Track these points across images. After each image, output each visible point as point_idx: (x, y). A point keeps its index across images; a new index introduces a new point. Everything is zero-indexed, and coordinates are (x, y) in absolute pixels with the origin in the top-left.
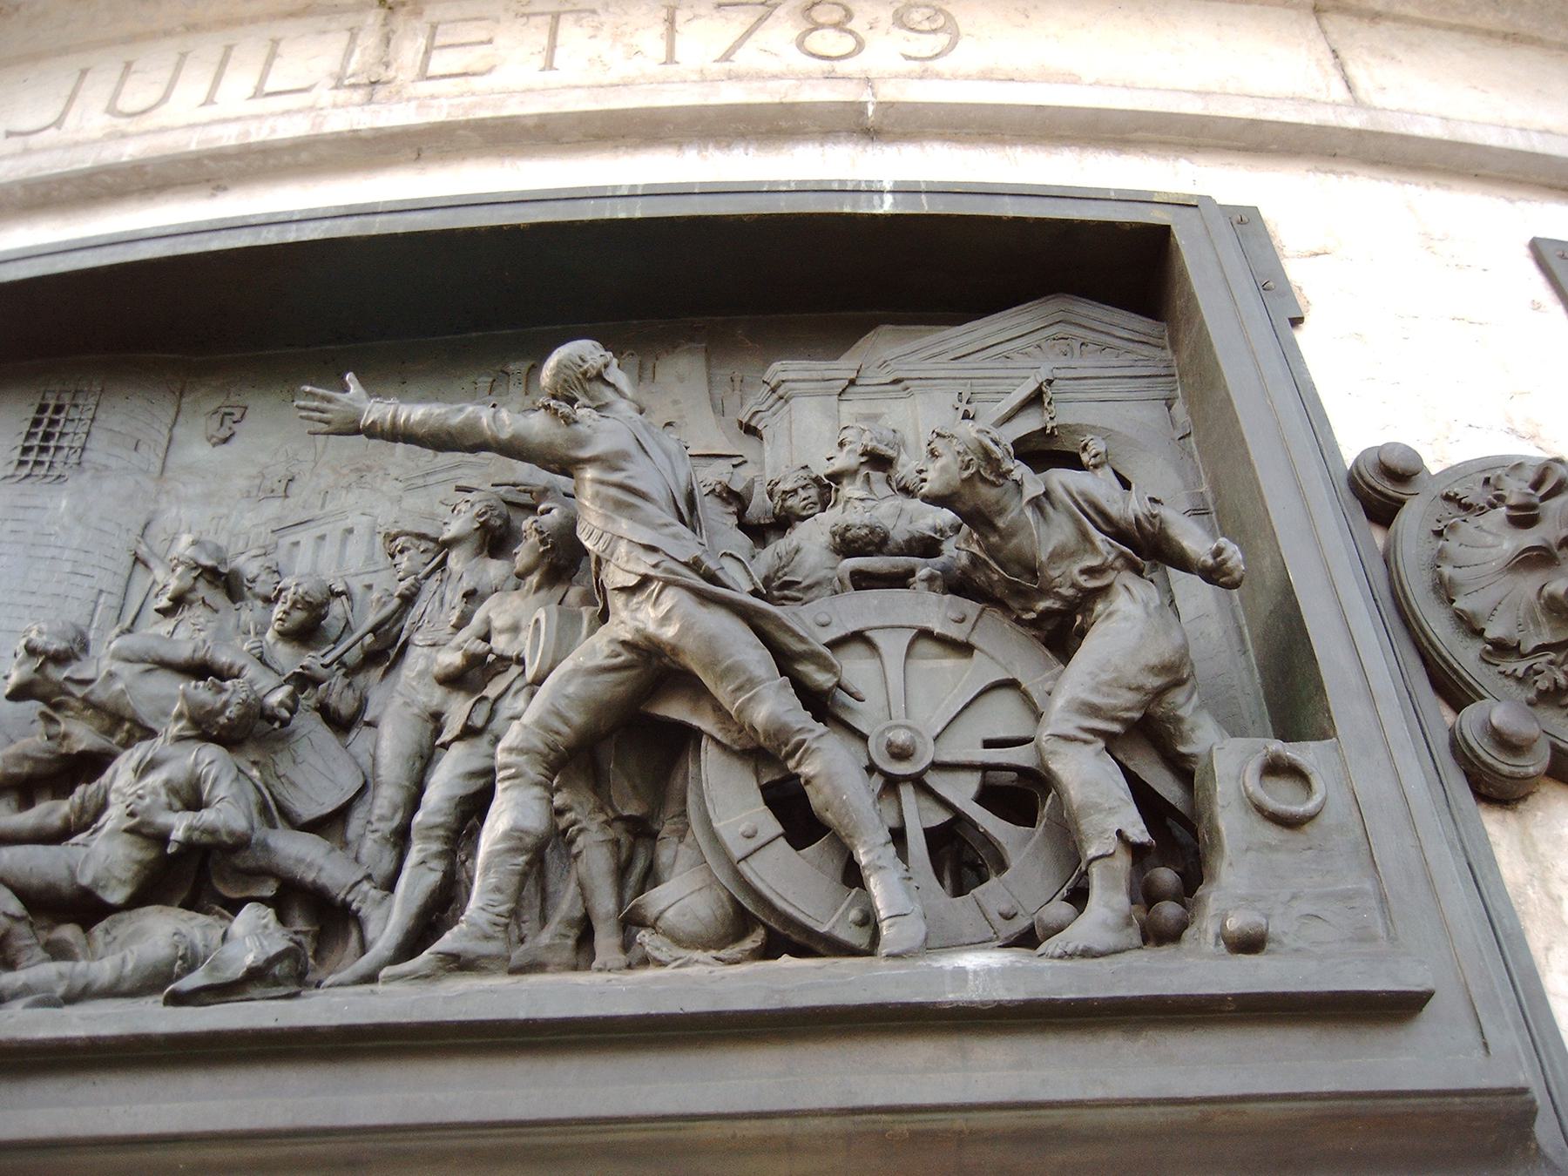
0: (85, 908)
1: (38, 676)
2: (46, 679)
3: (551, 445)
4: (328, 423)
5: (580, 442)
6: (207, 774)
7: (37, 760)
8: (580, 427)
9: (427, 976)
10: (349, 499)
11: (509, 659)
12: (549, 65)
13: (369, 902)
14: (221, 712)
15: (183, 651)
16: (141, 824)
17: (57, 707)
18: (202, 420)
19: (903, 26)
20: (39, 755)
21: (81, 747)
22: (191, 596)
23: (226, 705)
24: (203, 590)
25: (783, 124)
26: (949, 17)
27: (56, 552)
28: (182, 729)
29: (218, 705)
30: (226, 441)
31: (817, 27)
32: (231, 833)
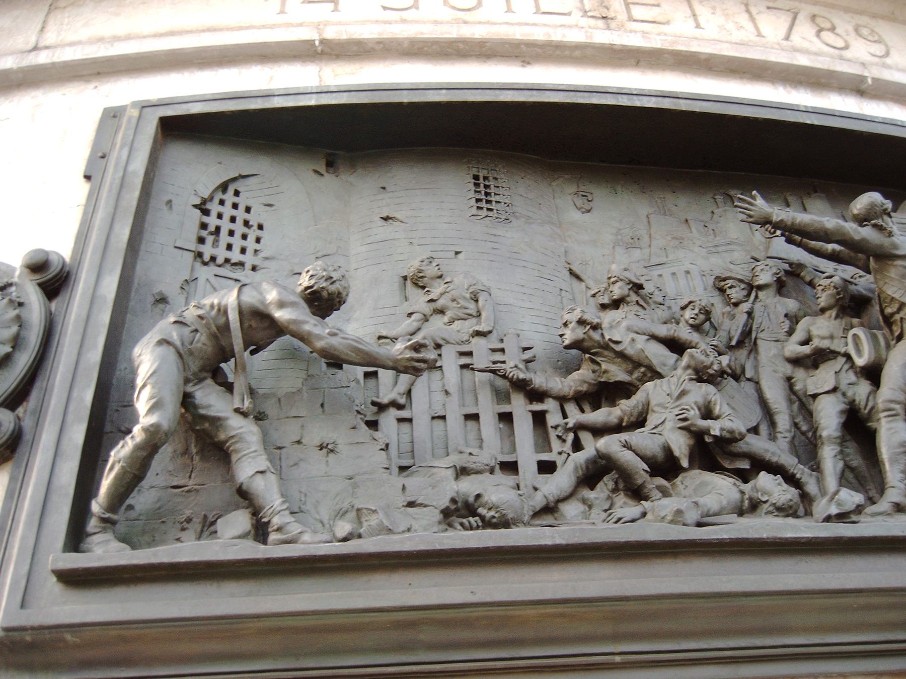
0: (666, 467)
2: (591, 338)
3: (881, 246)
4: (750, 216)
5: (895, 247)
6: (716, 400)
7: (590, 384)
8: (893, 238)
9: (889, 514)
10: (681, 253)
11: (838, 353)
12: (698, 26)
13: (806, 475)
14: (710, 367)
15: (663, 331)
16: (692, 425)
18: (569, 198)
19: (860, 36)
21: (618, 379)
22: (628, 299)
23: (712, 364)
24: (634, 297)
25: (823, 80)
26: (880, 36)
27: (525, 264)
28: (689, 375)
29: (709, 363)
30: (589, 211)
31: (820, 30)
32: (740, 433)
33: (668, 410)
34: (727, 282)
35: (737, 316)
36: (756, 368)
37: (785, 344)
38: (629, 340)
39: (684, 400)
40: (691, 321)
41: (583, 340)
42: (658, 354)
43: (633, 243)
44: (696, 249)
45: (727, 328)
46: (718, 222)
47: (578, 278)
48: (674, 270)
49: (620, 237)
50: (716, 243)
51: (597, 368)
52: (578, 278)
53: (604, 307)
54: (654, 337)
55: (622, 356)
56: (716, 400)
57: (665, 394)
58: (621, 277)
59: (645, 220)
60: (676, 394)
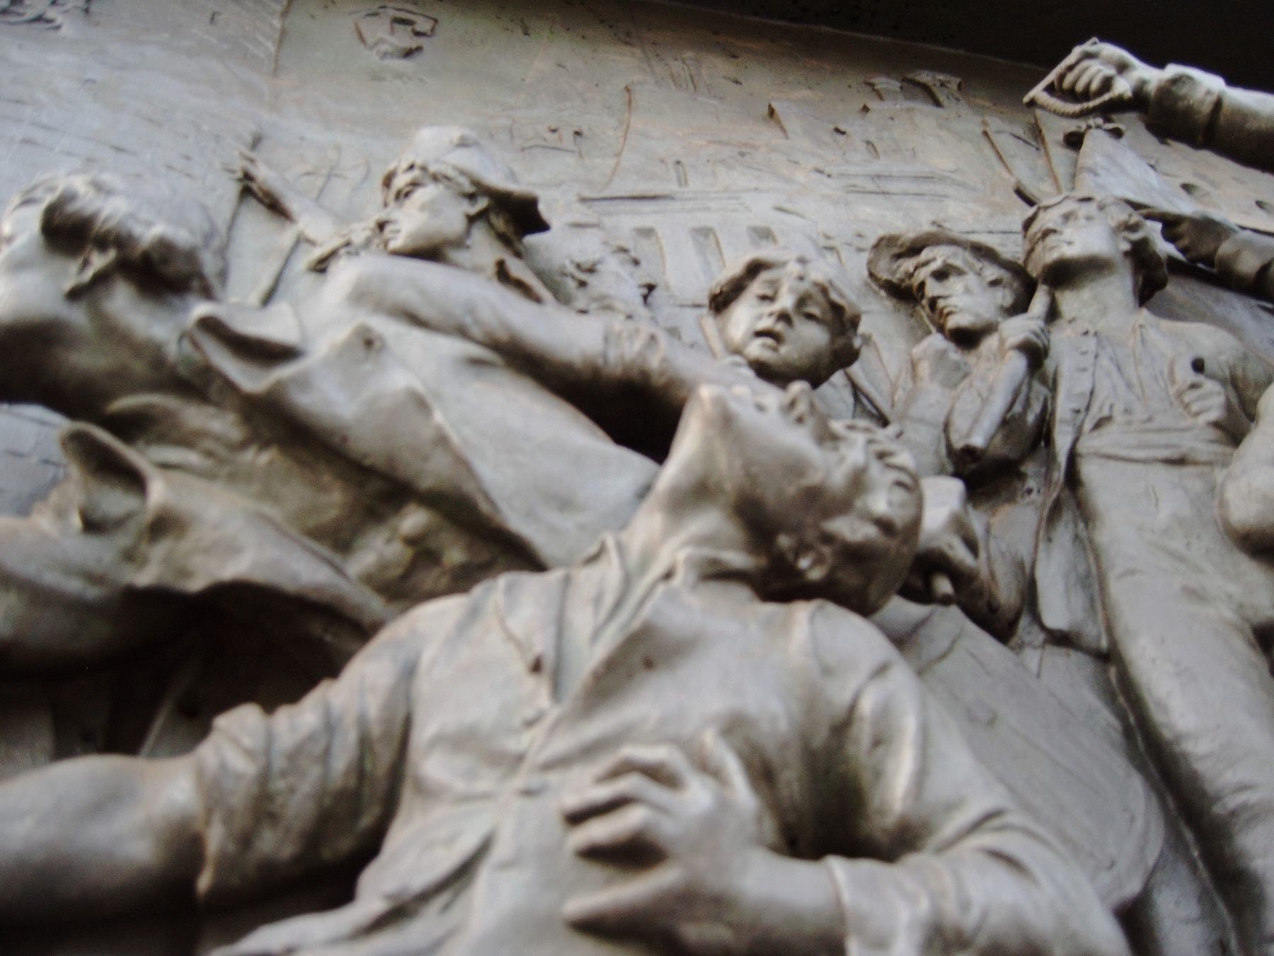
1: (77, 316)
2: (110, 332)
6: (885, 713)
10: (739, 178)
14: (843, 505)
16: (689, 899)
17: (133, 426)
20: (52, 578)
23: (858, 482)
30: (408, 53)
33: (521, 780)
34: (925, 254)
36: (1093, 582)
37: (1219, 475)
39: (646, 704)
40: (757, 349)
42: (521, 447)
51: (115, 501)
52: (275, 207)
55: (286, 430)
56: (885, 713)
57: (519, 667)
60: (589, 655)
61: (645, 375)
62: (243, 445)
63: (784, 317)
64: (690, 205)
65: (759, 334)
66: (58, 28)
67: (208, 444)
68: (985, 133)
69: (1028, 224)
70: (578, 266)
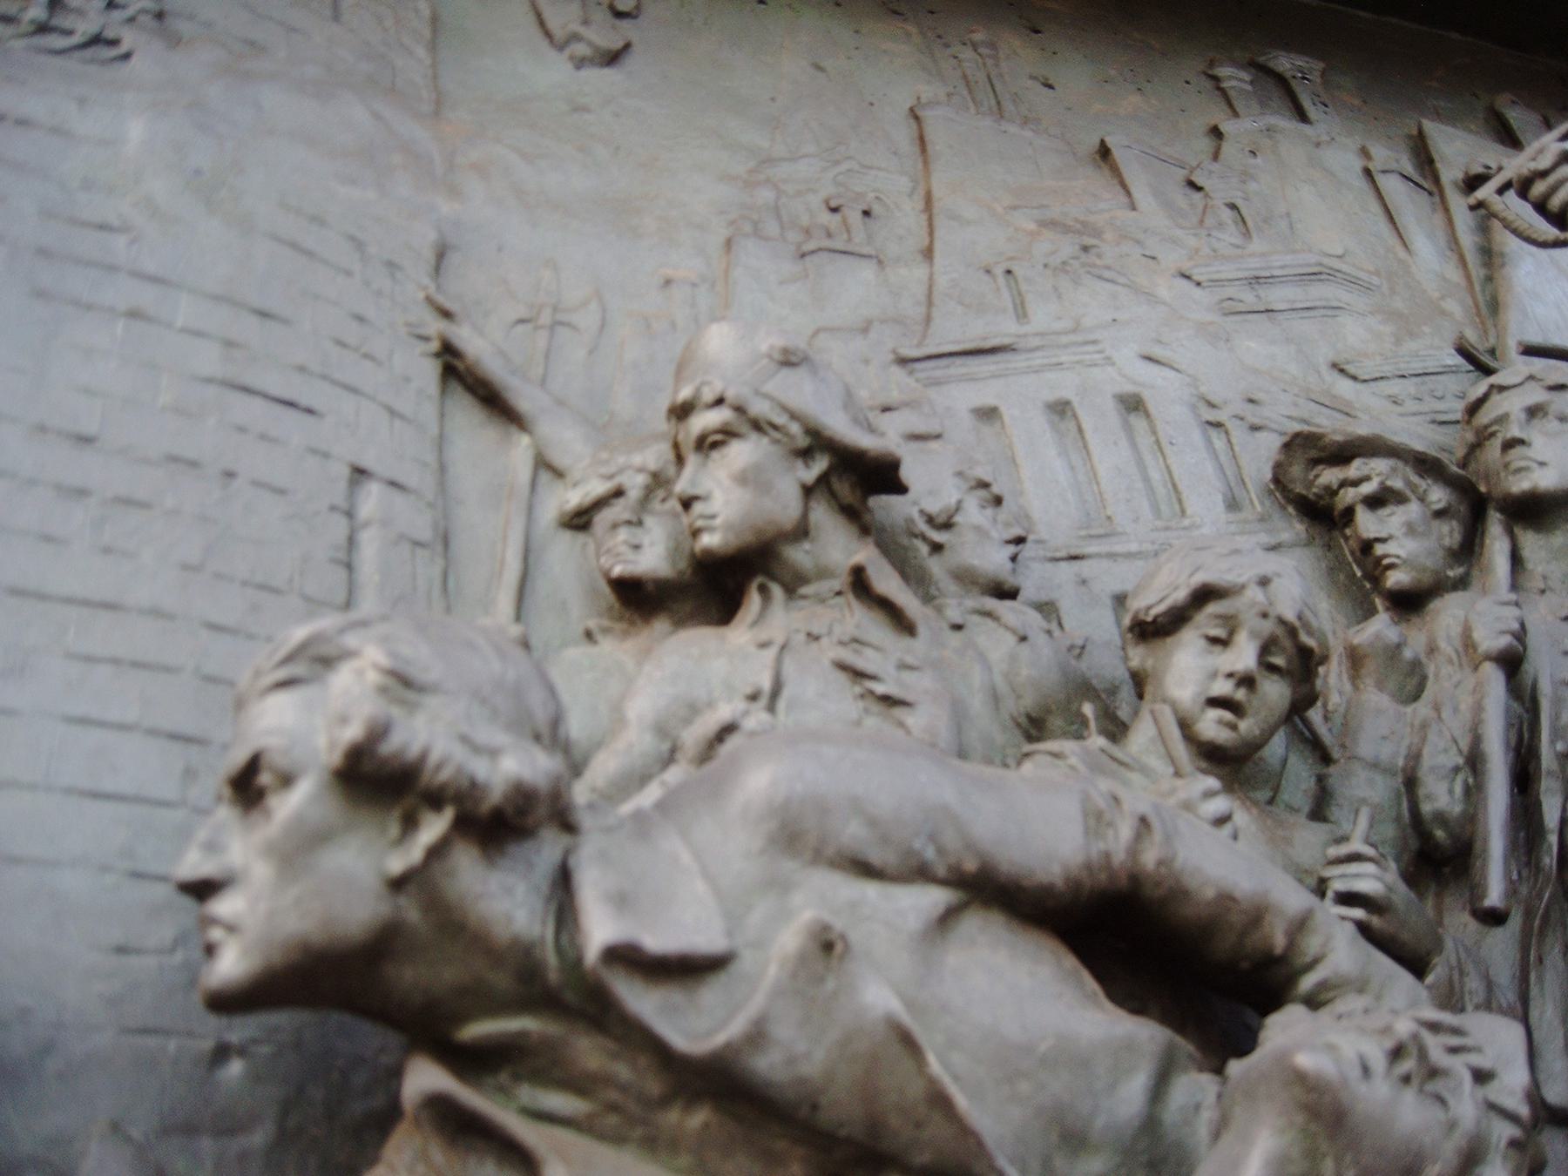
2: (453, 926)
10: (1091, 303)
22: (798, 555)
24: (836, 546)
27: (146, 296)
30: (612, 58)
34: (1355, 469)
35: (1445, 678)
38: (790, 939)
40: (1211, 725)
41: (384, 943)
43: (835, 233)
44: (1168, 288)
45: (1394, 753)
46: (1246, 176)
47: (494, 402)
48: (1064, 385)
49: (766, 195)
50: (1253, 265)
52: (494, 402)
53: (637, 599)
54: (990, 891)
58: (759, 408)
59: (903, 136)
61: (1136, 879)
62: (665, 1102)
63: (1247, 681)
64: (1038, 359)
65: (1214, 702)
66: (127, 56)
67: (613, 1095)
68: (1368, 173)
69: (1474, 408)
70: (930, 520)
